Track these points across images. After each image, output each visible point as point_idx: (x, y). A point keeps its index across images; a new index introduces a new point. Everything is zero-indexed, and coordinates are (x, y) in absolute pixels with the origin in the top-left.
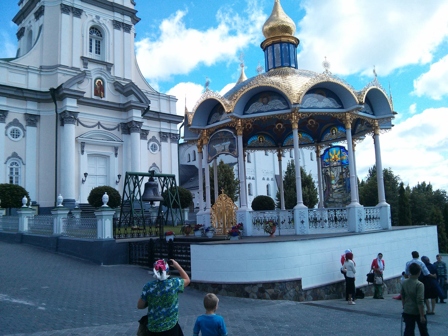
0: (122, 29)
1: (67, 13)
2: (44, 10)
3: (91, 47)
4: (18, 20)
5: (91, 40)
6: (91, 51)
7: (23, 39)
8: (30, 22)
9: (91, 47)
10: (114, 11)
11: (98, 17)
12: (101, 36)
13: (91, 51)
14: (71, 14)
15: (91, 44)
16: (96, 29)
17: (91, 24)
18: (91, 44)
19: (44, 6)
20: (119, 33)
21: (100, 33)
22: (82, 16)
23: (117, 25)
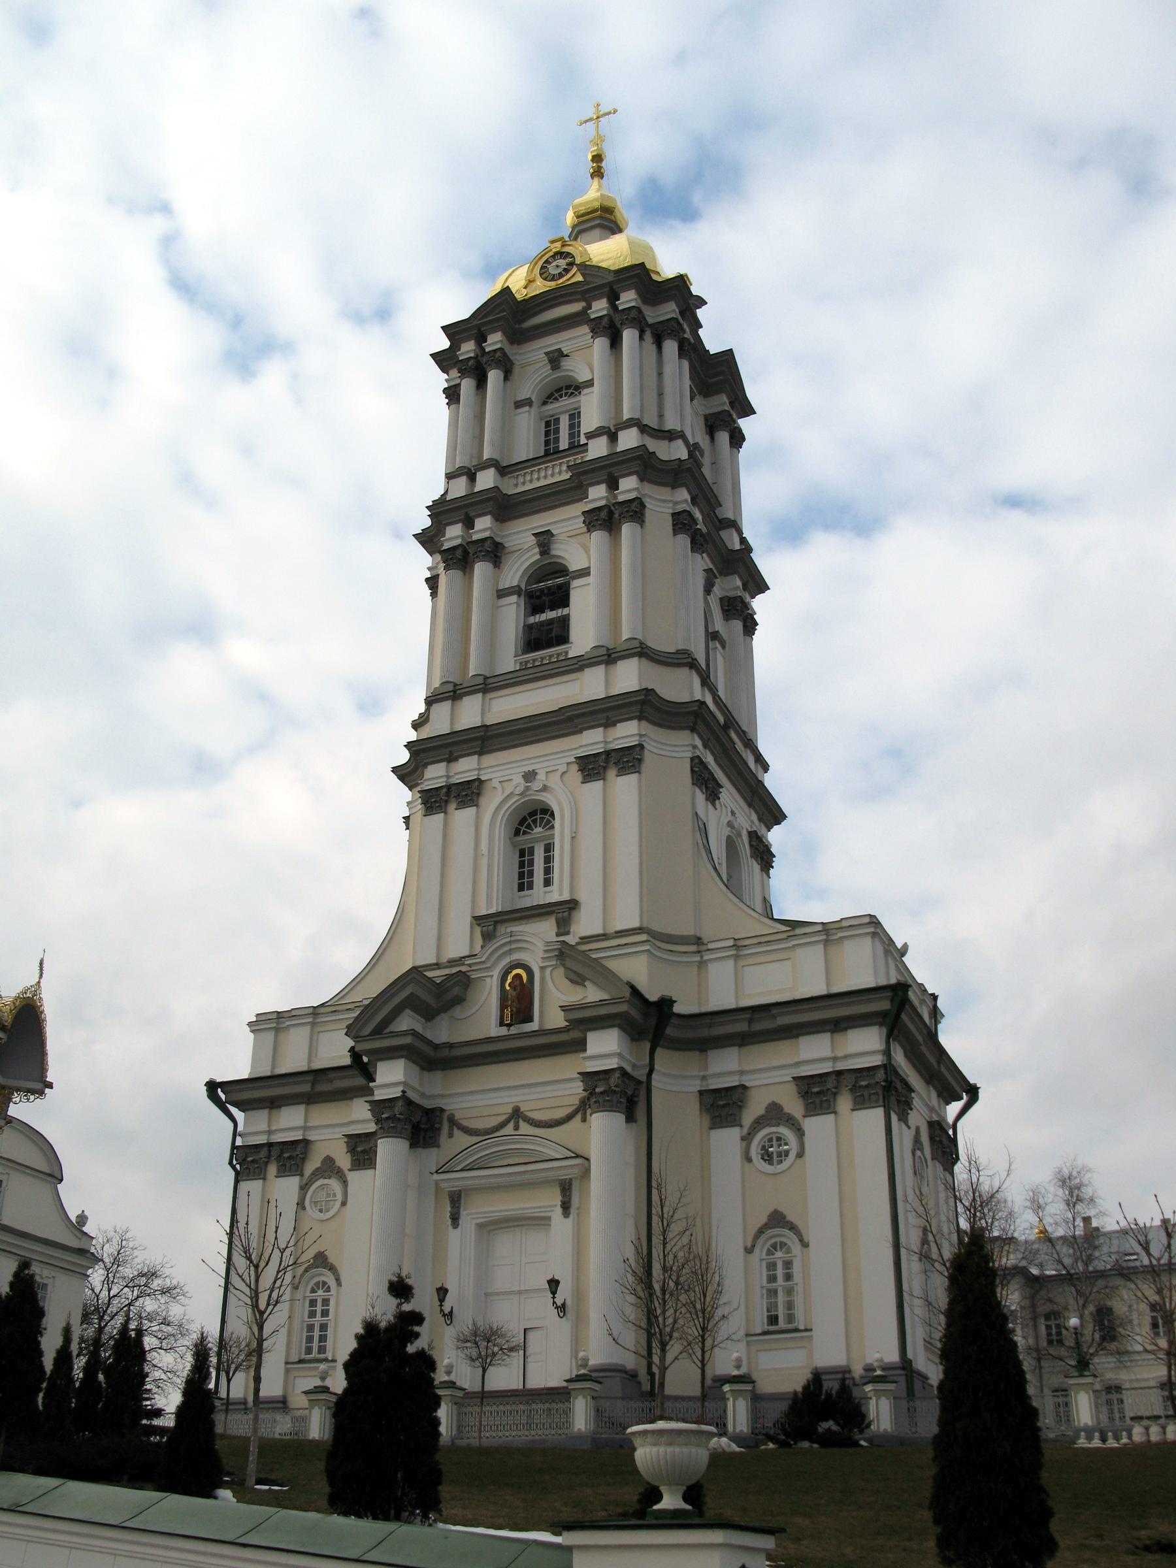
2: (640, 760)
7: (462, 817)
8: (530, 776)
10: (750, 805)
19: (641, 746)
20: (757, 867)
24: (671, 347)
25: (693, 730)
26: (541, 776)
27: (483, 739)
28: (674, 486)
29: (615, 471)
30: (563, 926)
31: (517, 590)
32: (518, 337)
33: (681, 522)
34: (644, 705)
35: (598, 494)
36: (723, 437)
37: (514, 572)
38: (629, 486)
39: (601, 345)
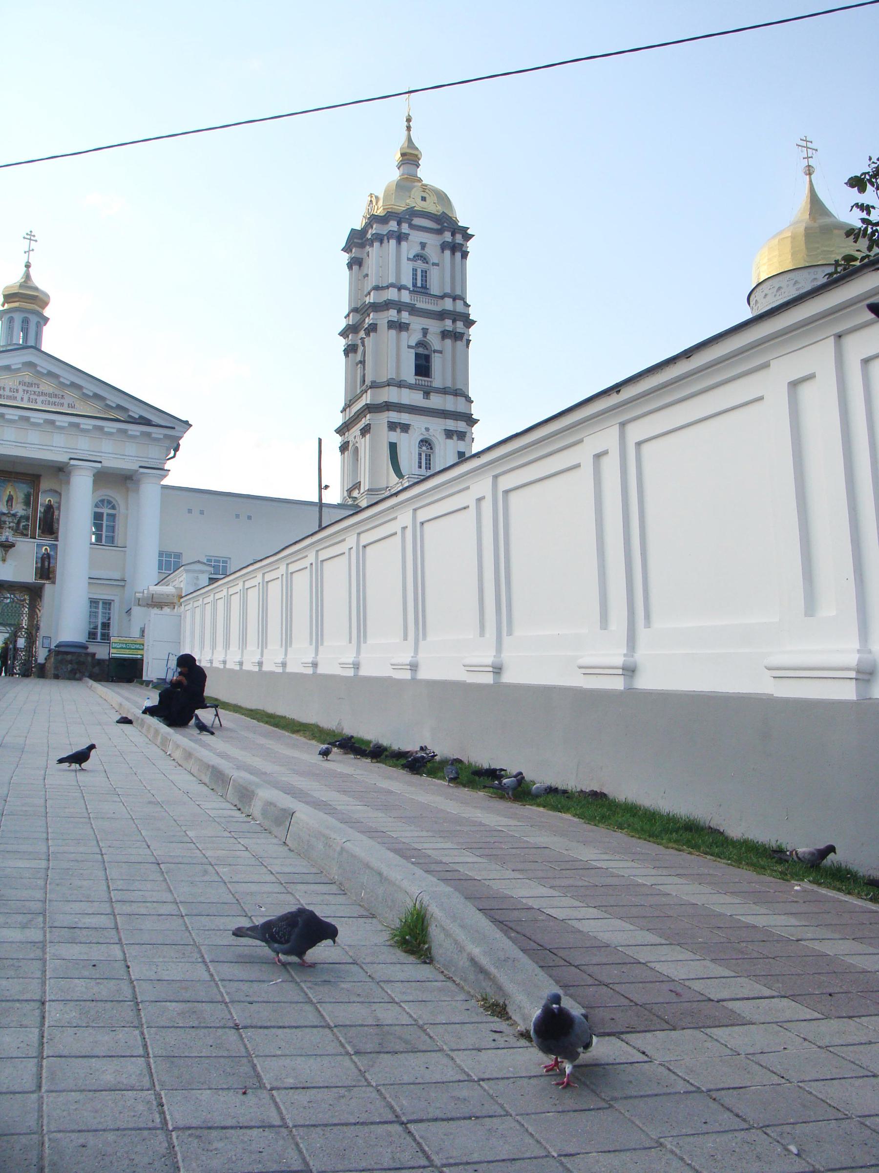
0: (455, 438)
1: (395, 431)
3: (420, 463)
4: (340, 431)
5: (420, 454)
6: (420, 467)
7: (346, 453)
9: (420, 463)
11: (427, 429)
12: (431, 449)
13: (420, 467)
14: (398, 430)
15: (420, 459)
16: (426, 442)
17: (421, 437)
18: (420, 459)
21: (430, 444)
22: (410, 431)
23: (449, 434)
24: (393, 242)
25: (388, 410)
26: (357, 439)
27: (347, 426)
28: (388, 310)
29: (369, 311)
30: (359, 490)
31: (360, 362)
32: (362, 246)
33: (391, 325)
34: (370, 408)
35: (367, 320)
36: (448, 253)
37: (359, 357)
38: (371, 315)
39: (370, 250)
